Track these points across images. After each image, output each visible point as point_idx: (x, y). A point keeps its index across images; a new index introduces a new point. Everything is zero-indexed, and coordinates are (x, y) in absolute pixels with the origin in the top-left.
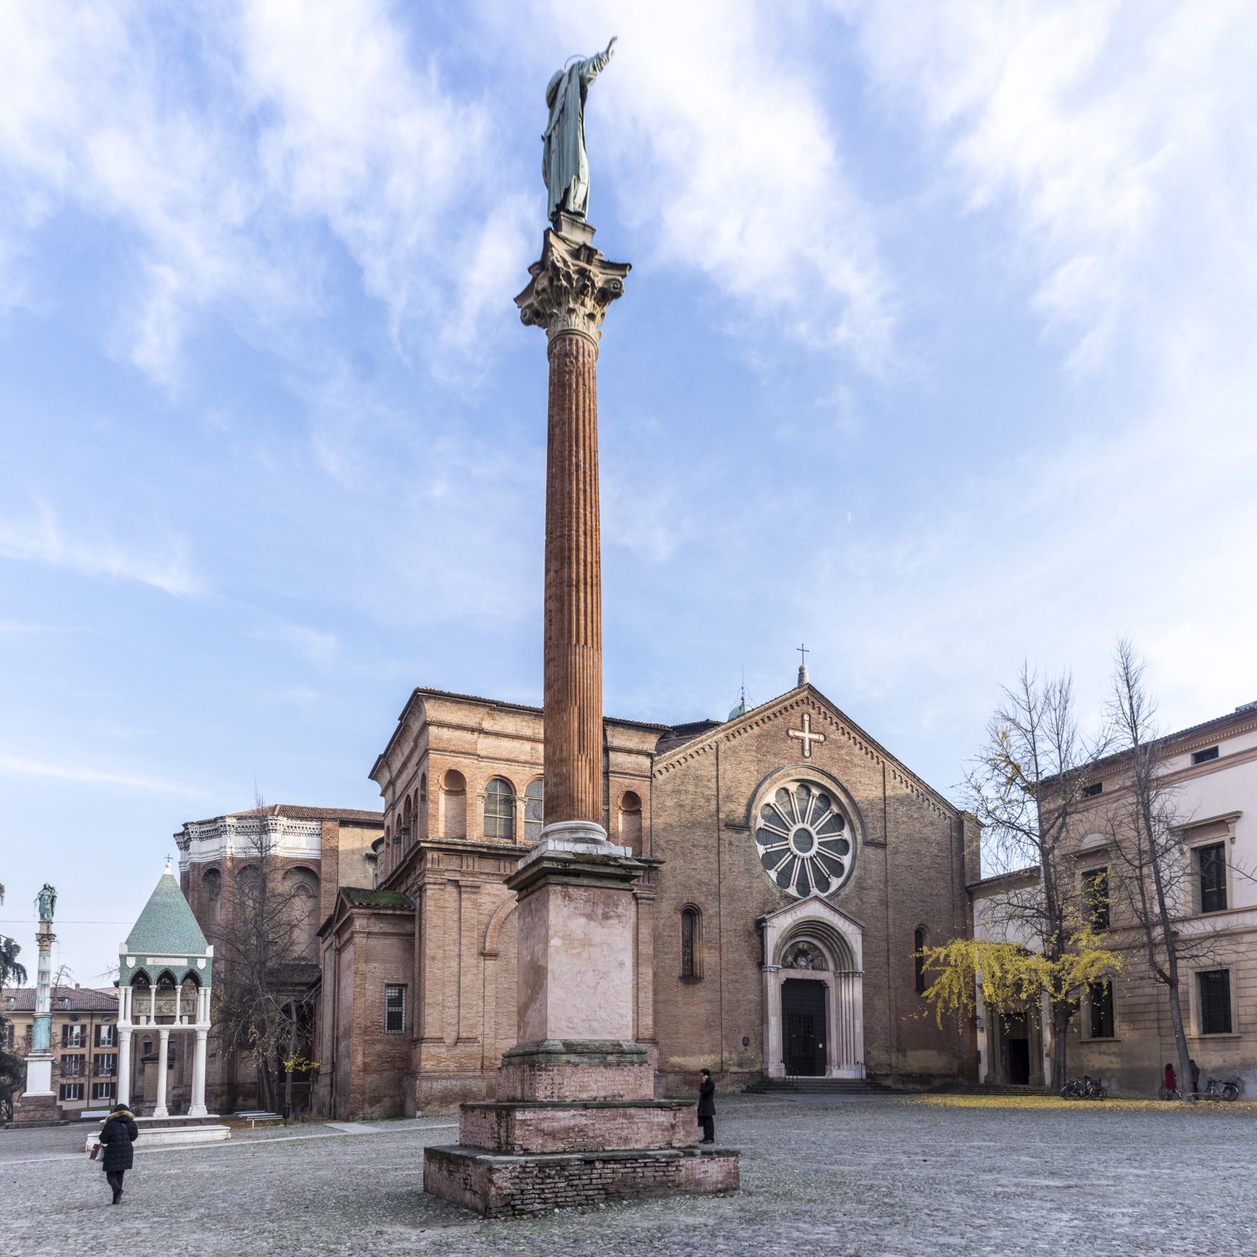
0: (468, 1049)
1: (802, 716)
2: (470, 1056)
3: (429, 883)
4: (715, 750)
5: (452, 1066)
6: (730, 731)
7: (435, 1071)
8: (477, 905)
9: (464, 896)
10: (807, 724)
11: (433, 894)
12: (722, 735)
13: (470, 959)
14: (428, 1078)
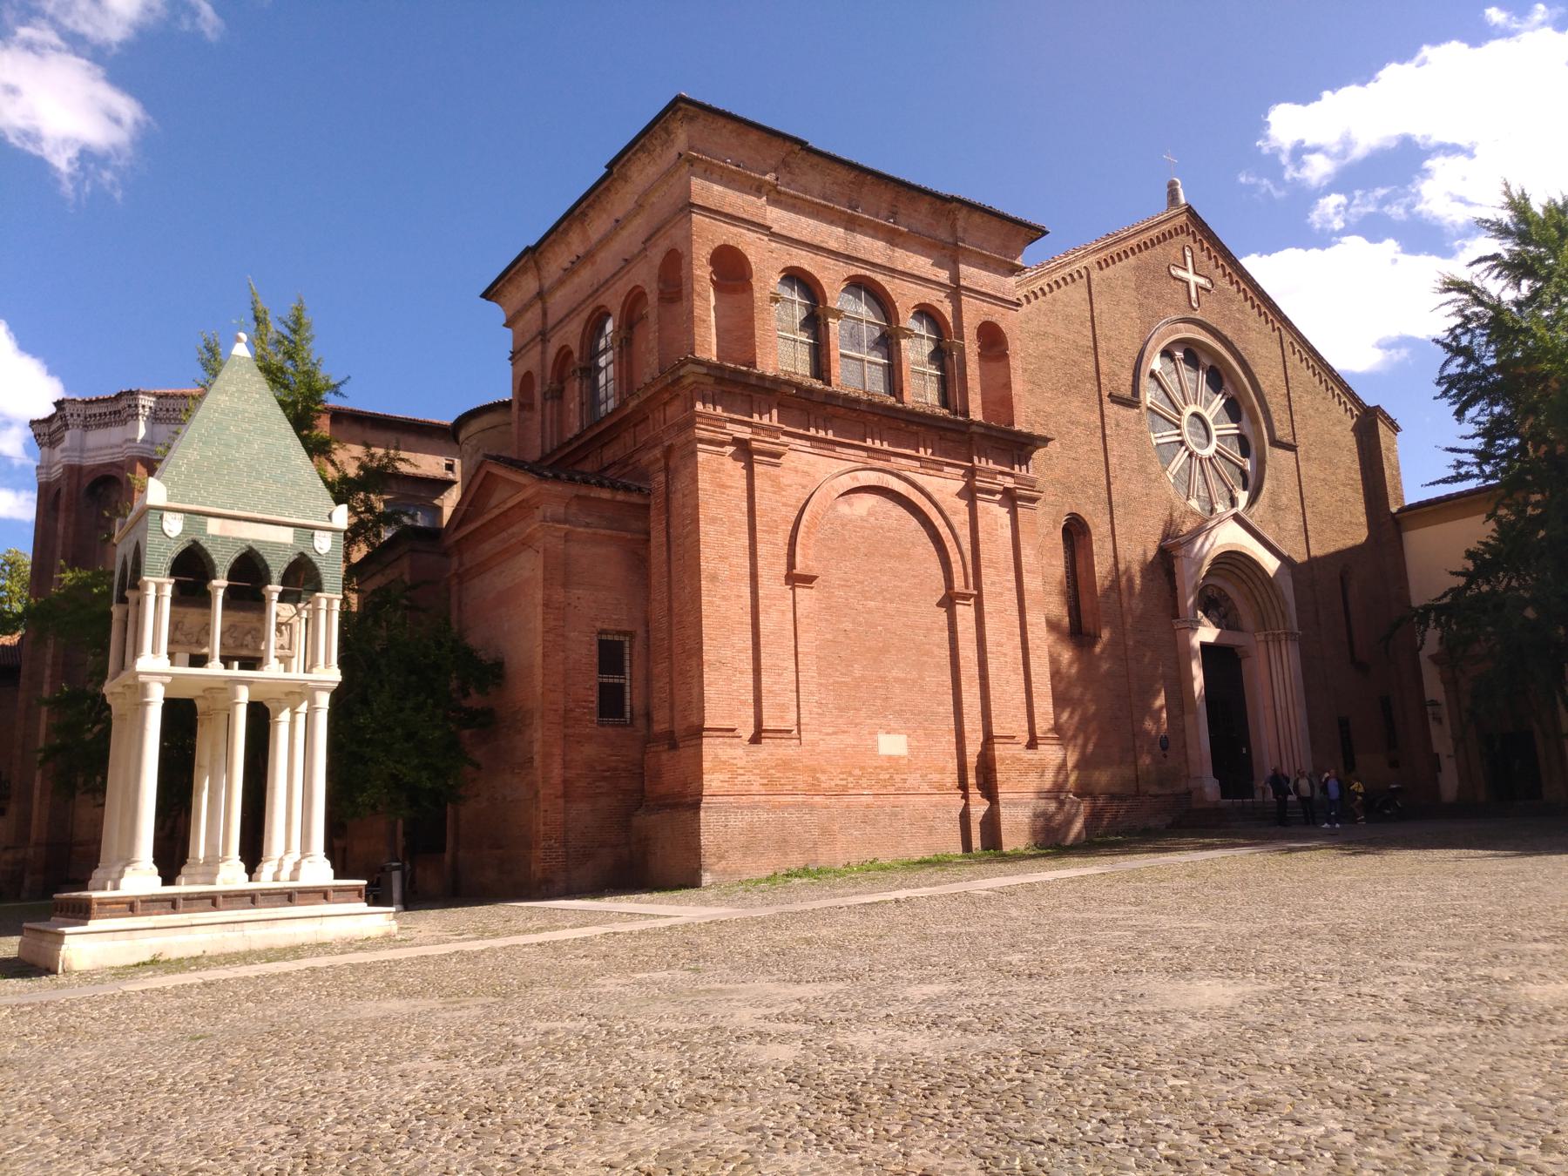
1: (1184, 249)
2: (785, 765)
3: (701, 441)
4: (1085, 277)
6: (1102, 255)
8: (778, 487)
9: (758, 468)
10: (1189, 260)
11: (708, 461)
12: (1092, 259)
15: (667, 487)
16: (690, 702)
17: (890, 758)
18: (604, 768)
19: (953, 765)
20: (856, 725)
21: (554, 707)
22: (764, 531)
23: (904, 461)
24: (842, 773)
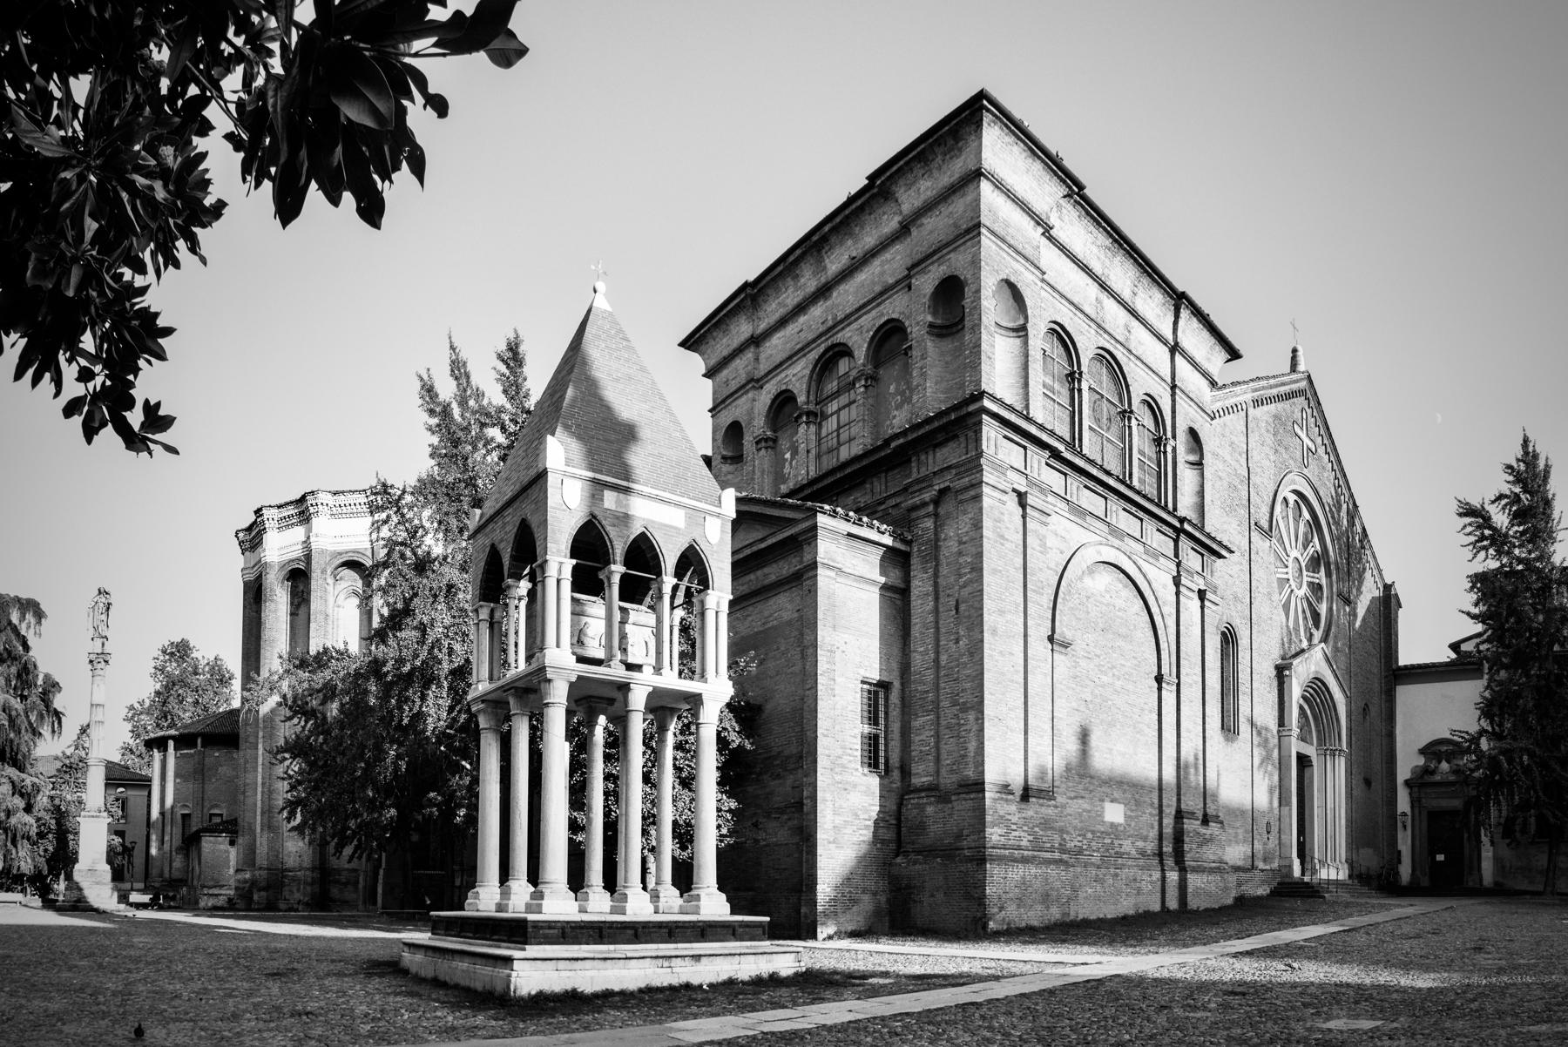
0: (1043, 810)
2: (1046, 824)
8: (1044, 549)
9: (1031, 525)
13: (1039, 647)
14: (1001, 859)
15: (936, 533)
16: (964, 756)
17: (1112, 824)
18: (867, 817)
19: (1154, 833)
20: (1091, 791)
21: (827, 752)
22: (1034, 591)
24: (1079, 835)
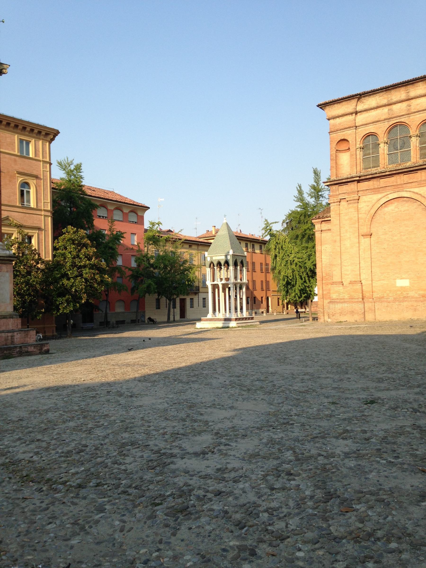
5: (346, 296)
7: (338, 299)
11: (334, 208)
17: (402, 287)
23: (410, 185)
